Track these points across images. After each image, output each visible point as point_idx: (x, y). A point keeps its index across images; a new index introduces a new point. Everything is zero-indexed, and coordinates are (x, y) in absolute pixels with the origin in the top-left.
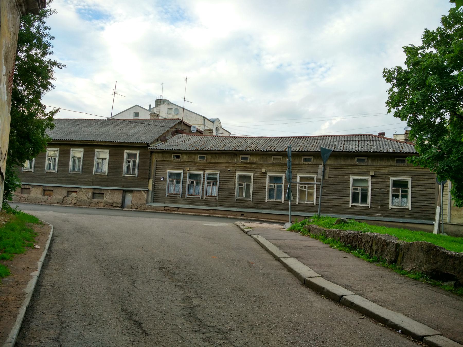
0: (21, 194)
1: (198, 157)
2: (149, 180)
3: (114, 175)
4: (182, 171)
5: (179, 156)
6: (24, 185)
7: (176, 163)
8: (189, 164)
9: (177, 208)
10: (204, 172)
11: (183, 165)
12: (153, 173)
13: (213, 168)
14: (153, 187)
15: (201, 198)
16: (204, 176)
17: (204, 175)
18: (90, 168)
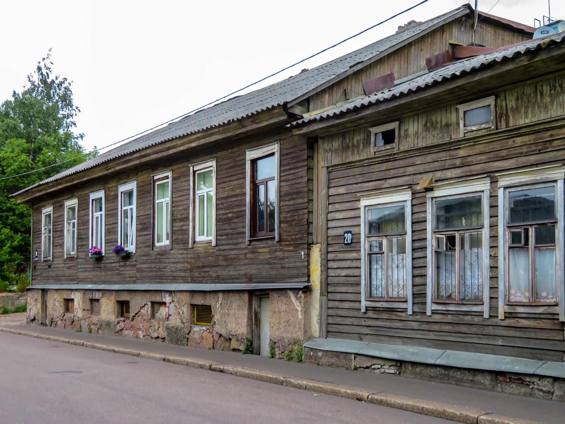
0: (92, 313)
1: (461, 114)
2: (309, 249)
3: (230, 242)
4: (406, 196)
5: (393, 131)
6: (92, 291)
7: (385, 166)
8: (429, 158)
9: (397, 361)
10: (494, 181)
11: (410, 170)
12: (319, 220)
13: (533, 159)
14: (324, 276)
15: (486, 315)
16: (493, 207)
17: (493, 197)
18: (184, 228)
